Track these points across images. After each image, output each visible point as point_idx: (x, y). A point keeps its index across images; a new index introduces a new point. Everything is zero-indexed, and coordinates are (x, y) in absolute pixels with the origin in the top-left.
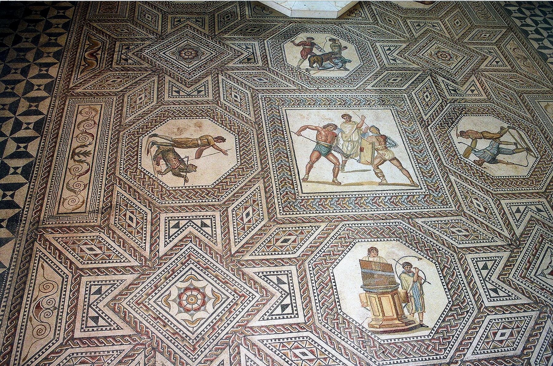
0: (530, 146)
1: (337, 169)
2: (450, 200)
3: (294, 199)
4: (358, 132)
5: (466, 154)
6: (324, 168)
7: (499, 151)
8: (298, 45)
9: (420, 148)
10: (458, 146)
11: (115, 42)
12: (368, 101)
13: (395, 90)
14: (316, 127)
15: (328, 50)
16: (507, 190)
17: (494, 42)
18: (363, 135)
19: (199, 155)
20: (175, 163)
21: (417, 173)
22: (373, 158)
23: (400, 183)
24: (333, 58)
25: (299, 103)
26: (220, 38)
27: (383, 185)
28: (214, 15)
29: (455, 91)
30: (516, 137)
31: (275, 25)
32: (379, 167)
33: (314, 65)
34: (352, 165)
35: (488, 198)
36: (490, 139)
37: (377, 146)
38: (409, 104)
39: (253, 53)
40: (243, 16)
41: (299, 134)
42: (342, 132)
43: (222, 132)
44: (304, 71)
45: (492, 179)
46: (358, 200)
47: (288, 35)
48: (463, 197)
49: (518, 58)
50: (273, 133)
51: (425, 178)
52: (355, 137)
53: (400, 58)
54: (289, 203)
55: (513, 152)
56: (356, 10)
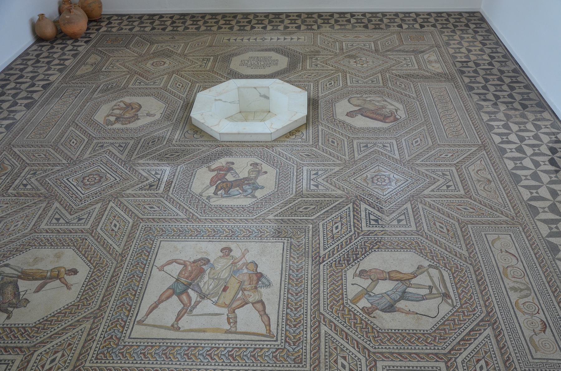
0: (451, 290)
1: (184, 311)
2: (308, 356)
3: (116, 345)
4: (231, 268)
5: (355, 300)
7: (404, 296)
8: (213, 170)
9: (299, 289)
11: (26, 167)
12: (261, 232)
13: (301, 220)
14: (185, 261)
15: (243, 174)
16: (393, 348)
17: (455, 162)
18: (234, 272)
21: (280, 320)
22: (233, 300)
23: (252, 331)
25: (182, 234)
27: (231, 333)
29: (376, 221)
32: (236, 311)
34: (207, 306)
35: (361, 357)
36: (397, 280)
37: (247, 285)
38: (310, 236)
39: (159, 179)
40: (170, 140)
41: (161, 269)
42: (213, 267)
44: (205, 198)
45: (378, 332)
46: (191, 350)
47: (206, 160)
48: (327, 354)
49: (479, 181)
50: (133, 267)
51: (288, 327)
52: (225, 275)
53: (325, 183)
54: (108, 348)
55: (424, 298)
56: (299, 131)
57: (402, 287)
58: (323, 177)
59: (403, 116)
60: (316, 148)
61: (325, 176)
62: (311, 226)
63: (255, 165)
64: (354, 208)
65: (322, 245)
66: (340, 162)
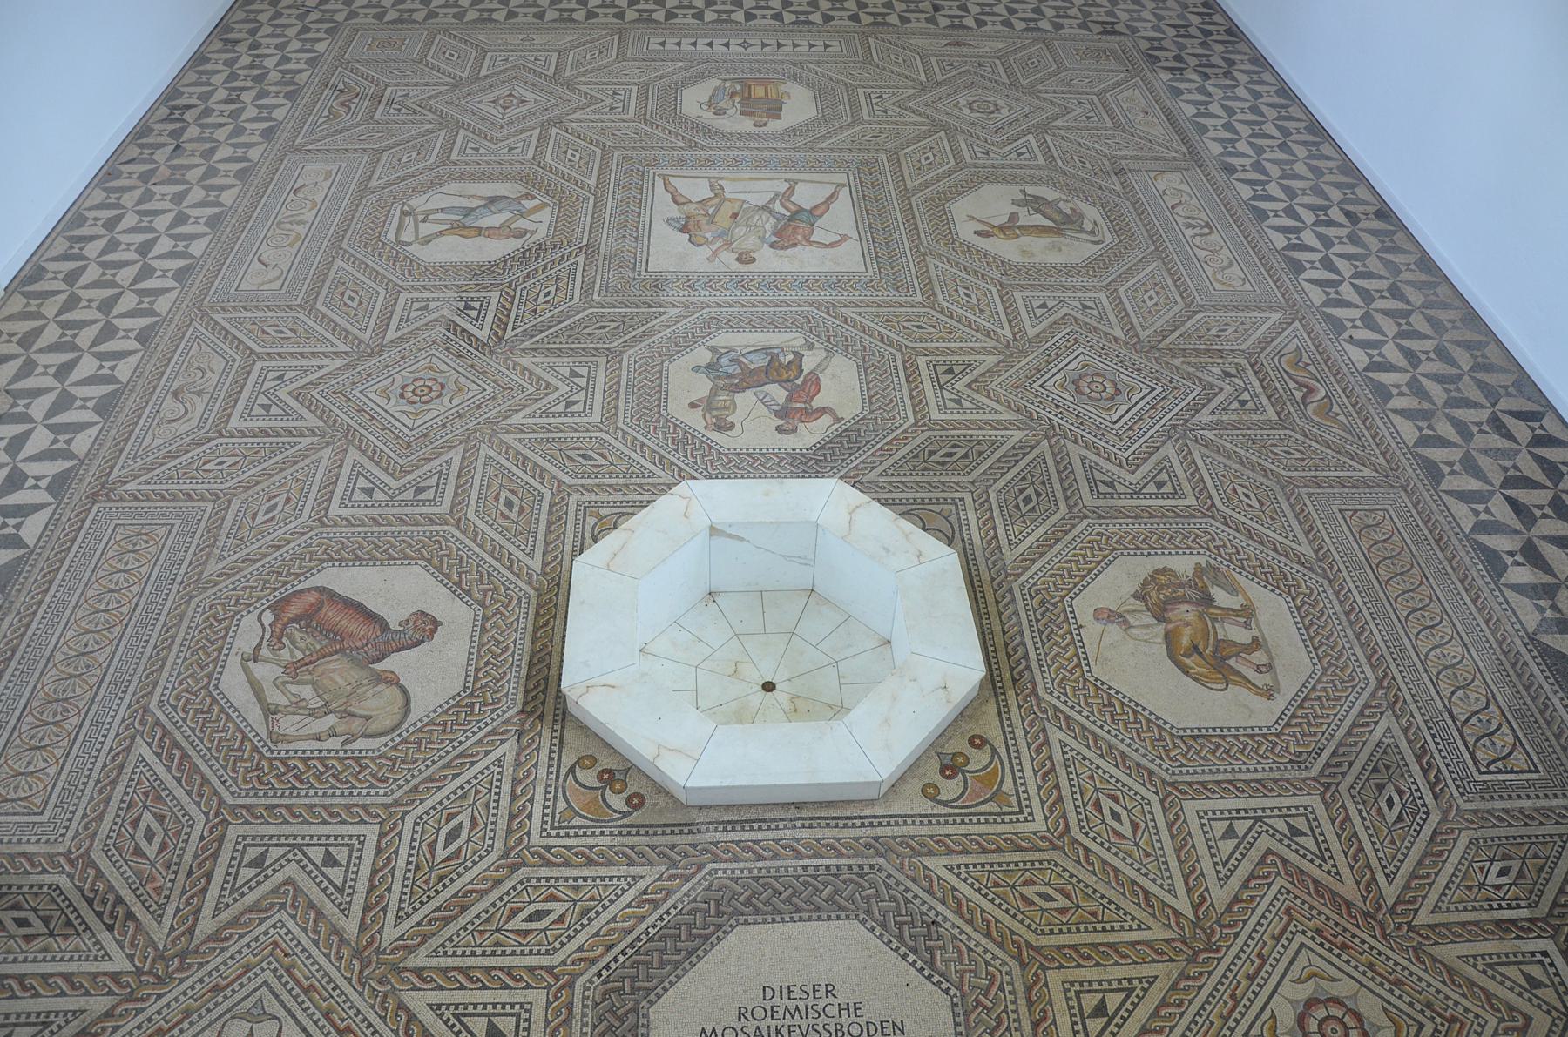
6: (807, 196)
7: (469, 211)
8: (823, 410)
10: (546, 219)
19: (1013, 217)
20: (1049, 211)
24: (735, 377)
26: (1031, 429)
28: (1070, 508)
29: (468, 307)
30: (411, 228)
31: (884, 474)
33: (790, 357)
39: (941, 387)
41: (844, 238)
42: (763, 239)
43: (982, 243)
57: (468, 221)
58: (556, 395)
59: (249, 621)
60: (561, 482)
61: (551, 398)
62: (596, 297)
63: (723, 427)
64: (505, 330)
65: (580, 269)
66: (507, 438)
